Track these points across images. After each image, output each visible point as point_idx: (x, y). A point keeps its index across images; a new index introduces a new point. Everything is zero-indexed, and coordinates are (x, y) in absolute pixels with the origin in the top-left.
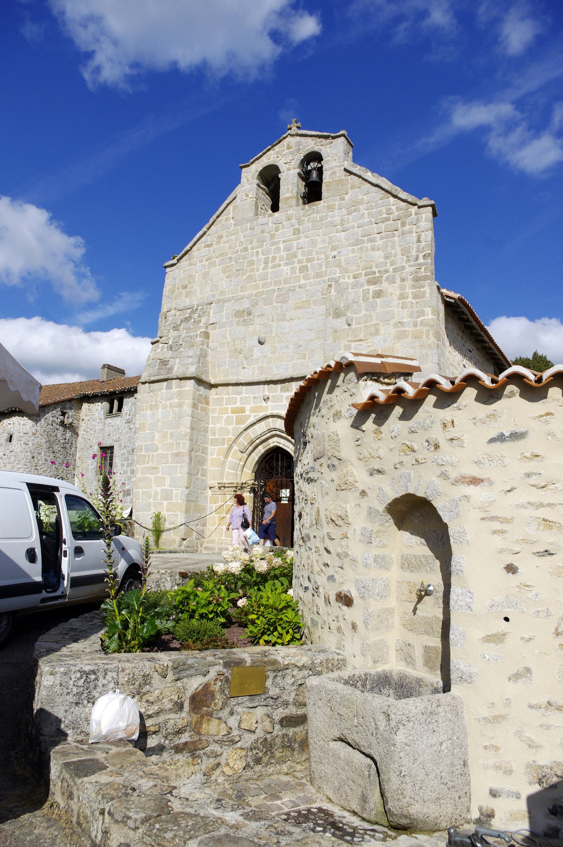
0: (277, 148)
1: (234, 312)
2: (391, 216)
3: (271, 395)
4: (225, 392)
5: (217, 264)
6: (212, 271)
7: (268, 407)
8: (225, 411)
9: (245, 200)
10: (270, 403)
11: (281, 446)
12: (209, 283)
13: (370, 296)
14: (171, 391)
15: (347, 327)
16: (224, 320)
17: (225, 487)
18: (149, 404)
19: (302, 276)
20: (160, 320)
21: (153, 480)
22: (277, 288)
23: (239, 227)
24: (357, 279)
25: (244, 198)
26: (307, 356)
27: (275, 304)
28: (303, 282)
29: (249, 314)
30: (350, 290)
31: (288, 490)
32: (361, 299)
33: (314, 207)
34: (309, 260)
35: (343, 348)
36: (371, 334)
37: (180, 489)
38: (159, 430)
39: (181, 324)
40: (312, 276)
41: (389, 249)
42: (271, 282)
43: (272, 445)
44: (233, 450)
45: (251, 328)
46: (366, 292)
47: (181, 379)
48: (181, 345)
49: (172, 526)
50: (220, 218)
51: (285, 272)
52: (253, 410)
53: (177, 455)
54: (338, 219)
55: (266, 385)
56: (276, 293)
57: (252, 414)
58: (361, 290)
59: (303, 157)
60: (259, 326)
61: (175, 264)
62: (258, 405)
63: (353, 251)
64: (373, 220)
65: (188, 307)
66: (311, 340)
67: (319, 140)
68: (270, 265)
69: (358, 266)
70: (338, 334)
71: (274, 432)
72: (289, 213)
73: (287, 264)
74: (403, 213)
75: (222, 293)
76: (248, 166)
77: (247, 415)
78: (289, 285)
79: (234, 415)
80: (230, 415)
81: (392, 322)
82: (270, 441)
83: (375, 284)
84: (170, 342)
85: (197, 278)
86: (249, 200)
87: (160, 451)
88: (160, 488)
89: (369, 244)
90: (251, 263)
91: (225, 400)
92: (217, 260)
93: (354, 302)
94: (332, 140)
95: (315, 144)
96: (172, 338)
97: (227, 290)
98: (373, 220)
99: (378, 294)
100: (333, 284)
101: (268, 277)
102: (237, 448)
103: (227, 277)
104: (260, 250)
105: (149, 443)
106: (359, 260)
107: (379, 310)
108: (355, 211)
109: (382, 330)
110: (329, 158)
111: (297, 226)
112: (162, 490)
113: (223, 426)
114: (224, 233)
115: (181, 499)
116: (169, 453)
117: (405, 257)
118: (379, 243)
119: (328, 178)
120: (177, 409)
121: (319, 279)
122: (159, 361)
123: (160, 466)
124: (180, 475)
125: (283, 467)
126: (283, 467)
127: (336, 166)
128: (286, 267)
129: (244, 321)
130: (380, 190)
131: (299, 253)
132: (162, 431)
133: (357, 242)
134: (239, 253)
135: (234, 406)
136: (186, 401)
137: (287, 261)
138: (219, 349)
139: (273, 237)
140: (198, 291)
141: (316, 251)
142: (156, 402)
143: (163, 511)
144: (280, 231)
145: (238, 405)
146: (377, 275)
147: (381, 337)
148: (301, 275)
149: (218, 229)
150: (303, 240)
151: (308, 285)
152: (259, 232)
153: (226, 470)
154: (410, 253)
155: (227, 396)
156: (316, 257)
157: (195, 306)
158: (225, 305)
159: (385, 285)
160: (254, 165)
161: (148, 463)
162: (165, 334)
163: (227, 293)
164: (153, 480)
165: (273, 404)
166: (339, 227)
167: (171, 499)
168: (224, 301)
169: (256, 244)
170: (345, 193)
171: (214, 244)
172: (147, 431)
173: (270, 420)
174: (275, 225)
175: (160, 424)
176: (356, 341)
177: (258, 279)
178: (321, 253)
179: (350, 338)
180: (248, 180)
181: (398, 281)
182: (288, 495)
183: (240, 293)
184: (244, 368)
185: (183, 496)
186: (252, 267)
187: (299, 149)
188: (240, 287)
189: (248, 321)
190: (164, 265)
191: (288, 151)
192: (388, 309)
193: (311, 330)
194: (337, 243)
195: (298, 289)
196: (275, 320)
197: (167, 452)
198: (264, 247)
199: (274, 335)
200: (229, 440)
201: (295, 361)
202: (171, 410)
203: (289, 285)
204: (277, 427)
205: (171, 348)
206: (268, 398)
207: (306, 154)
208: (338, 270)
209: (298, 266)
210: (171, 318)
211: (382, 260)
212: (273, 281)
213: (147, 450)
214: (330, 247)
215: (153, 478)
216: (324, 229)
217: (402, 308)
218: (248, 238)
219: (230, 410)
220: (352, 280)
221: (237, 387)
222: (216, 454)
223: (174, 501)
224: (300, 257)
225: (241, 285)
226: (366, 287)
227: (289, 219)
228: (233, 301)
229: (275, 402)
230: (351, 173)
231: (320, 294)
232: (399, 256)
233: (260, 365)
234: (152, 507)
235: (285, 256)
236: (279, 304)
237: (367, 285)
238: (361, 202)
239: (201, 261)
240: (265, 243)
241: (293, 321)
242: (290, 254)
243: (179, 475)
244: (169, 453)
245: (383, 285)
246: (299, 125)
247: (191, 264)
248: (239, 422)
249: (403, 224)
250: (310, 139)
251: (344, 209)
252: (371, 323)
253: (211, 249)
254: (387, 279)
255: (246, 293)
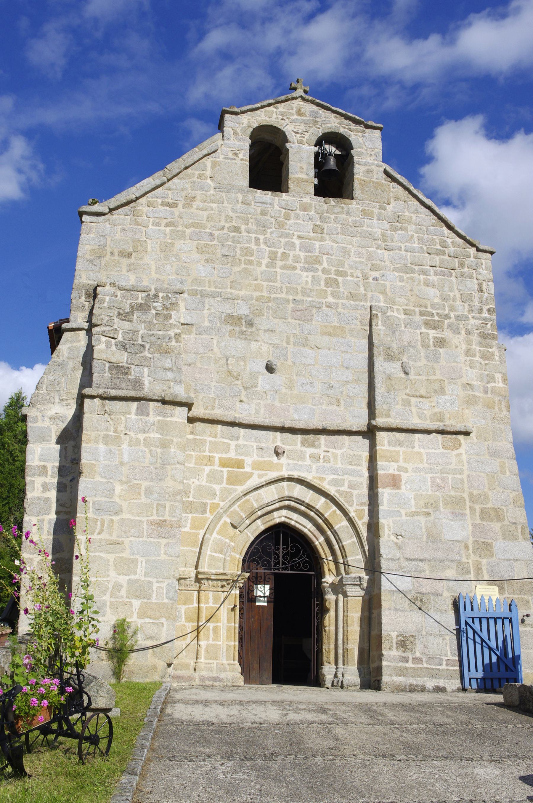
0: (281, 107)
1: (223, 315)
2: (446, 250)
3: (286, 447)
4: (208, 432)
5: (188, 237)
6: (179, 244)
7: (282, 465)
8: (210, 461)
9: (232, 159)
10: (284, 460)
11: (293, 523)
12: (173, 262)
13: (431, 343)
14: (147, 418)
15: (403, 375)
16: (206, 324)
17: (208, 579)
18: (102, 433)
19: (329, 293)
20: (74, 294)
21: (111, 563)
22: (291, 298)
23: (223, 194)
24: (410, 317)
25: (230, 155)
26: (342, 402)
27: (290, 320)
28: (330, 299)
29: (250, 324)
30: (403, 328)
31: (267, 587)
32: (419, 343)
33: (343, 205)
34: (339, 273)
35: (400, 402)
36: (435, 392)
37: (166, 582)
38: (124, 479)
39: (133, 313)
40: (345, 295)
41: (446, 289)
42: (281, 288)
43: (278, 521)
44: (222, 522)
45: (254, 346)
46: (425, 337)
47: (164, 402)
48: (143, 346)
49: (150, 643)
50: (189, 170)
51: (304, 279)
52: (257, 466)
53: (161, 524)
54: (378, 233)
55: (278, 433)
56: (291, 305)
57: (257, 472)
58: (418, 332)
59: (321, 134)
60: (267, 346)
61: (103, 214)
62: (266, 459)
63: (401, 279)
64: (425, 248)
65: (140, 289)
66: (347, 382)
67: (345, 121)
68: (279, 263)
69: (409, 300)
70: (393, 382)
71: (287, 503)
72: (305, 200)
73: (305, 269)
74: (461, 251)
75: (197, 281)
76: (236, 114)
77: (247, 472)
78: (311, 299)
79: (225, 470)
80: (216, 468)
81: (461, 382)
82: (276, 514)
83: (434, 328)
84: (120, 338)
85: (149, 247)
86: (238, 162)
87: (124, 516)
88: (127, 578)
89: (422, 277)
90: (248, 252)
91: (208, 444)
92: (188, 231)
93: (410, 344)
94: (364, 129)
95: (340, 124)
96: (121, 331)
97: (207, 279)
98: (425, 248)
99: (441, 343)
100: (379, 314)
101: (276, 278)
102: (229, 521)
103: (207, 261)
104: (261, 237)
105: (103, 499)
106: (410, 293)
107: (443, 362)
108: (401, 229)
109: (448, 388)
110: (362, 150)
111: (318, 223)
112: (129, 581)
113: (204, 483)
114: (199, 194)
115: (168, 598)
116: (145, 519)
117: (466, 305)
118: (433, 278)
119: (361, 174)
120: (159, 450)
121: (357, 303)
122: (108, 365)
123: (127, 541)
124: (167, 558)
125: (287, 554)
126: (287, 554)
127: (373, 164)
128: (304, 274)
129: (242, 333)
130: (432, 214)
131: (325, 261)
132: (129, 482)
133: (405, 269)
134: (226, 231)
135: (224, 456)
136: (175, 440)
137: (307, 266)
138: (199, 365)
139: (281, 225)
140: (153, 268)
141: (348, 264)
142: (115, 431)
143: (132, 616)
144: (292, 221)
145: (232, 455)
146: (436, 318)
147: (448, 398)
148: (329, 290)
149: (187, 186)
150: (328, 243)
151: (340, 306)
152: (259, 212)
153: (209, 553)
154: (472, 301)
155: (213, 439)
156: (349, 271)
157: (153, 289)
158: (207, 301)
159: (447, 334)
160: (244, 115)
161: (99, 533)
162: (105, 322)
163: (207, 284)
164: (111, 563)
165: (290, 462)
166: (379, 242)
167: (149, 597)
168: (204, 295)
169: (254, 227)
170: (386, 201)
171: (180, 205)
172: (98, 479)
173: (285, 484)
174: (284, 211)
175: (125, 470)
176: (417, 396)
177: (259, 277)
178: (357, 269)
179: (408, 391)
180: (236, 133)
181: (463, 332)
182: (268, 593)
183: (229, 290)
184: (241, 401)
185: (171, 594)
186: (249, 258)
187: (317, 122)
188: (229, 280)
189: (249, 334)
190: (81, 210)
191: (299, 118)
192: (454, 364)
193: (347, 368)
194: (379, 262)
195: (325, 308)
196: (292, 343)
197: (139, 518)
198: (268, 236)
199: (289, 363)
200: (215, 506)
201: (324, 407)
202: (146, 450)
203: (311, 299)
204: (295, 496)
205: (124, 347)
206: (284, 452)
207: (326, 131)
208: (381, 297)
209: (324, 277)
210: (107, 298)
211: (437, 300)
212: (284, 286)
213: (99, 510)
214: (370, 265)
215: (112, 560)
216: (359, 238)
217: (471, 367)
218: (239, 215)
219: (217, 461)
220: (403, 317)
221: (230, 428)
222: (189, 525)
223: (154, 600)
224: (325, 265)
225: (232, 278)
226: (424, 330)
227: (305, 208)
228: (219, 299)
229: (293, 459)
230: (394, 180)
231: (359, 323)
232: (459, 303)
233: (269, 402)
234: (108, 609)
235: (302, 257)
236: (297, 322)
237: (425, 328)
238: (409, 221)
239: (158, 224)
240: (269, 231)
241: (320, 351)
242: (311, 257)
243: (163, 557)
244: (145, 519)
245: (445, 333)
246: (307, 89)
247: (137, 223)
248: (233, 480)
249: (462, 265)
250: (332, 115)
251: (385, 222)
252: (435, 378)
253: (175, 210)
254: (450, 326)
255: (241, 293)
